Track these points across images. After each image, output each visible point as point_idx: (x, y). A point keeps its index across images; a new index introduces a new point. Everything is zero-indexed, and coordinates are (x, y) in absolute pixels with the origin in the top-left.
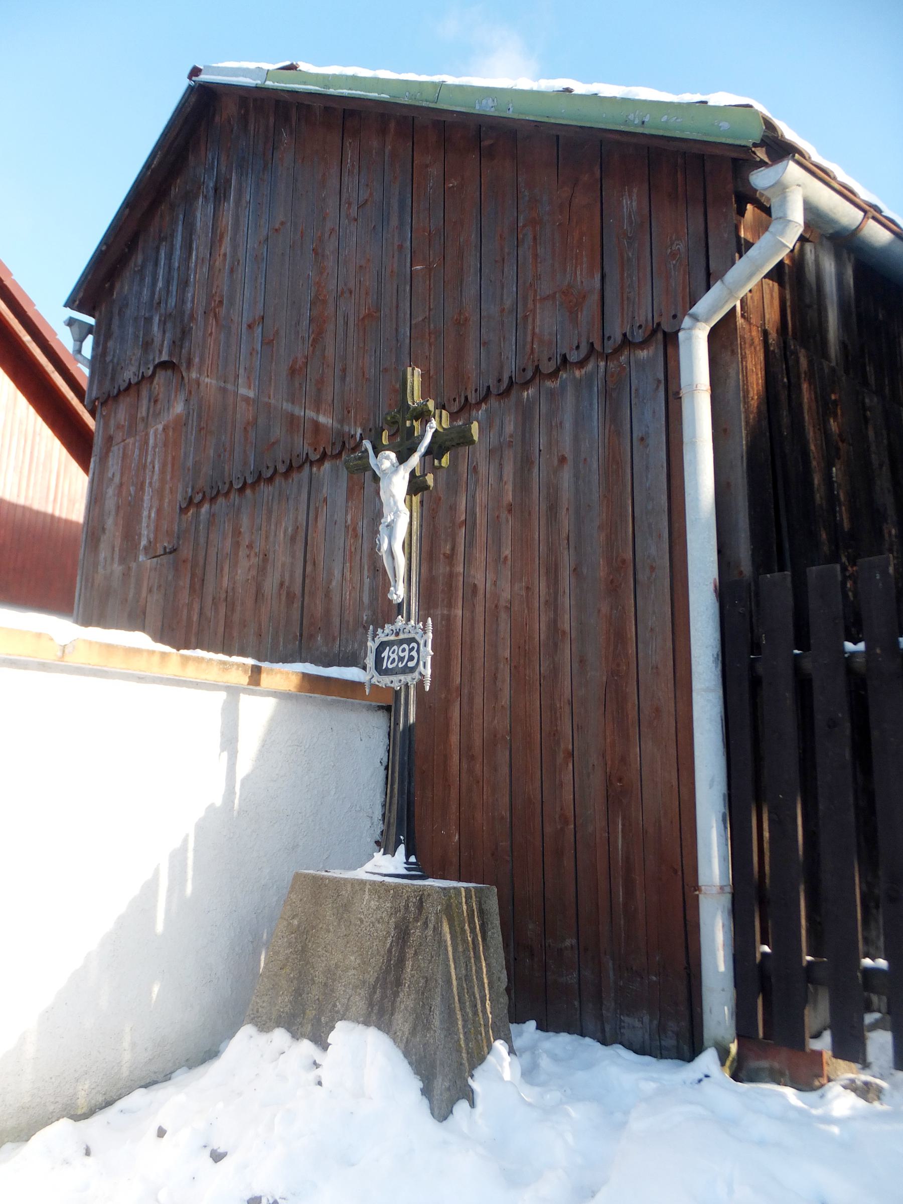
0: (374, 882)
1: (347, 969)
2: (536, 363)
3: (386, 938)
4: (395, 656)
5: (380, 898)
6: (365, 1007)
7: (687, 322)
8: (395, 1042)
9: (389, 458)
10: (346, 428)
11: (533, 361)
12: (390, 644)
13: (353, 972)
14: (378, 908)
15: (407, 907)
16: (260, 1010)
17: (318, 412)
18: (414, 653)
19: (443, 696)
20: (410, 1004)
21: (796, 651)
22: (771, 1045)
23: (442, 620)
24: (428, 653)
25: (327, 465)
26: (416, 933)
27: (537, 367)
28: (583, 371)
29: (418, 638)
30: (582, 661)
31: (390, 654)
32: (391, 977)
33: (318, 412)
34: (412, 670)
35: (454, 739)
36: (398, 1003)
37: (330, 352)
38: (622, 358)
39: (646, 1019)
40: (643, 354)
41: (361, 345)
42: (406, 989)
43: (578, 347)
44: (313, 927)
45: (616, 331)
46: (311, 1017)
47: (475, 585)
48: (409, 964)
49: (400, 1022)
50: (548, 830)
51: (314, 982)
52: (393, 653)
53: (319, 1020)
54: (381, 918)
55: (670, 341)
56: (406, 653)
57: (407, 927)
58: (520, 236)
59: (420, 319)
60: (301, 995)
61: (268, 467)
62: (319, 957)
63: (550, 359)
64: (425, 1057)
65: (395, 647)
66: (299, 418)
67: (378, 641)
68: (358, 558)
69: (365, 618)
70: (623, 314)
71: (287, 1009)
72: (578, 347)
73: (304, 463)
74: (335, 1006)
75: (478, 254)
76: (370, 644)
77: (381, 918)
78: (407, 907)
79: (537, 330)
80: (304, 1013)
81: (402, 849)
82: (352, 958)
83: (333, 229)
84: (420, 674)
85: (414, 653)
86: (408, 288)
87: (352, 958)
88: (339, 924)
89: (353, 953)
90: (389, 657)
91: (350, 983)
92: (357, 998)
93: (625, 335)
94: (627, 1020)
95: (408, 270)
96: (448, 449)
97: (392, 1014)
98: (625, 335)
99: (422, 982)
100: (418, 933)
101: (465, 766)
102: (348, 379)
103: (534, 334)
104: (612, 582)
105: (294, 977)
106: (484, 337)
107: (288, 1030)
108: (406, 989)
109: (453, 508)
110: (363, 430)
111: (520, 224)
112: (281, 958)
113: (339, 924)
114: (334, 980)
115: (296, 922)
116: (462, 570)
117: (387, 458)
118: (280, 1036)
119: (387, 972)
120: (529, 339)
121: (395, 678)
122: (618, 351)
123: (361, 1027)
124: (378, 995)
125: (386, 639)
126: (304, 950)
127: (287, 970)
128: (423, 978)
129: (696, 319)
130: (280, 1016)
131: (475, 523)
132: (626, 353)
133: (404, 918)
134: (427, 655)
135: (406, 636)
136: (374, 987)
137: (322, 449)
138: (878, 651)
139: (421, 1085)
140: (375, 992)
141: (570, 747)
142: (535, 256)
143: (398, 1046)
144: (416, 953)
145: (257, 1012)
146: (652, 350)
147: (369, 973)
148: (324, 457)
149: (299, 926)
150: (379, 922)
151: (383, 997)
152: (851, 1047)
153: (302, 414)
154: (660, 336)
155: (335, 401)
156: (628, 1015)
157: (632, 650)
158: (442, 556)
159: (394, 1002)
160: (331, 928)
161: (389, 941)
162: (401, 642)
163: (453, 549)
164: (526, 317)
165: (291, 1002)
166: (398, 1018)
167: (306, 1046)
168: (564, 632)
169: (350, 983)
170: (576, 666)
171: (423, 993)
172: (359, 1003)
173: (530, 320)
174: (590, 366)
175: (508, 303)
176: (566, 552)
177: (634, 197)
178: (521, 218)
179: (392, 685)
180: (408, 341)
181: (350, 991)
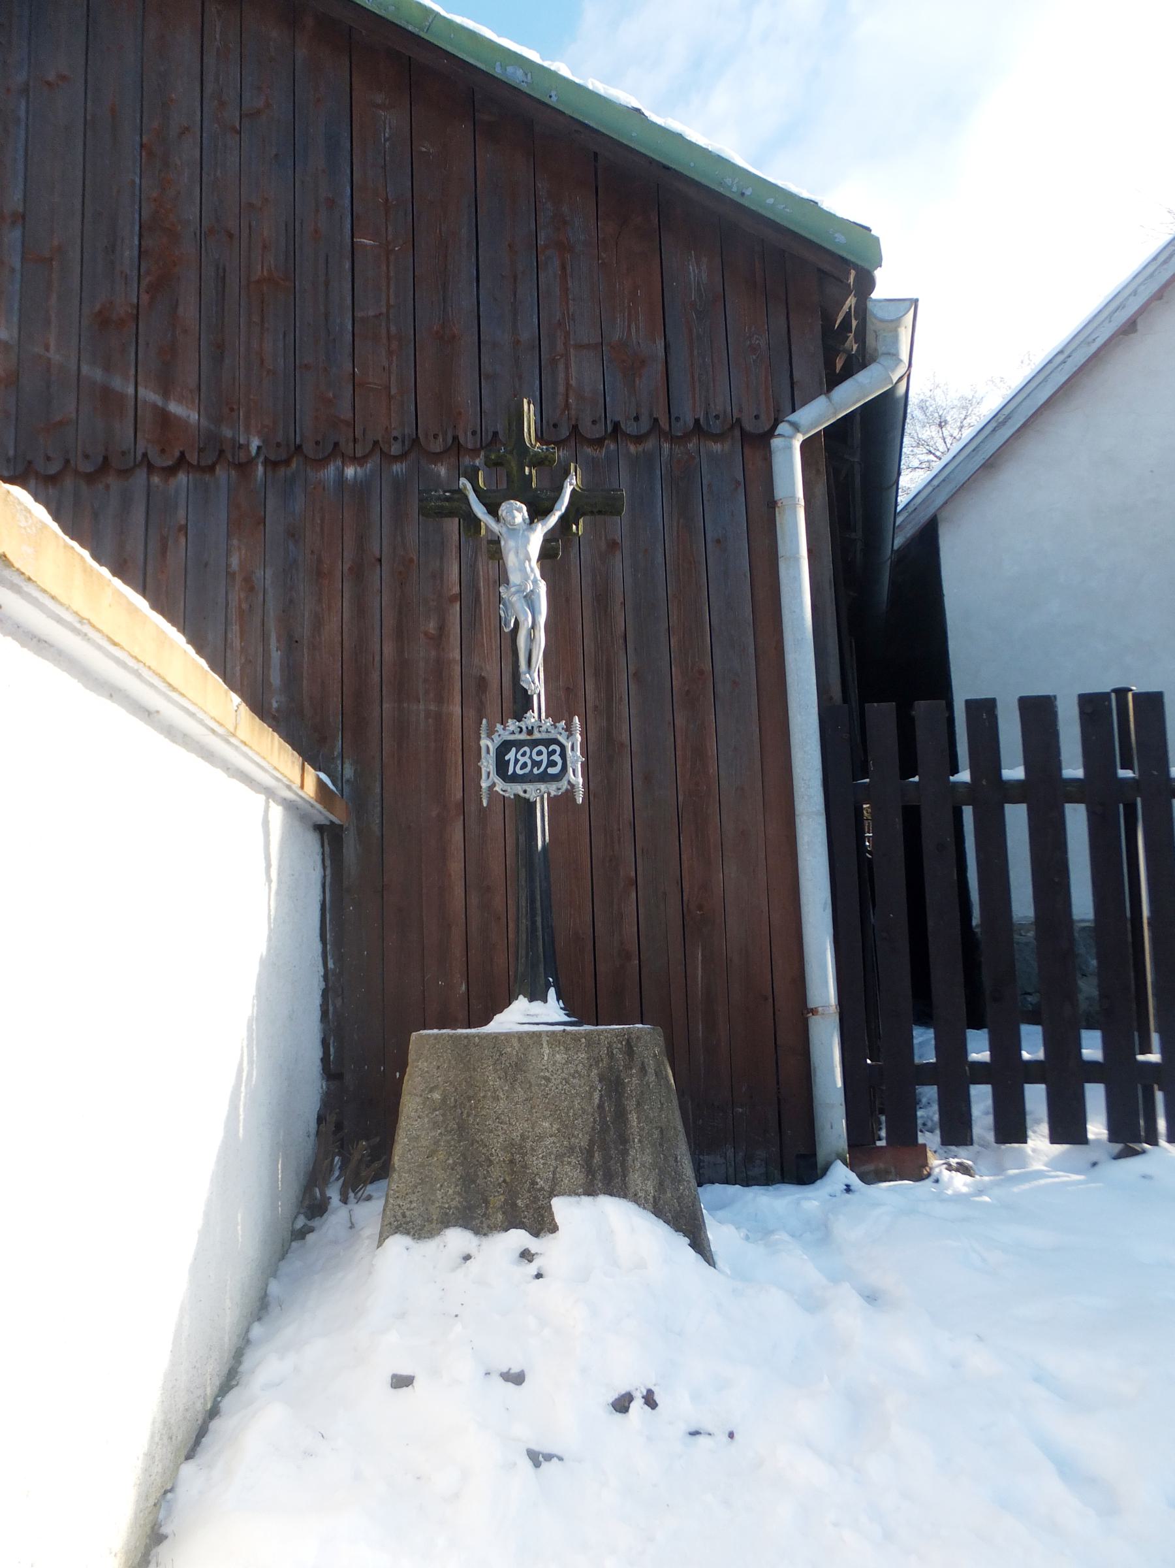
0: (553, 1032)
1: (541, 1138)
2: (573, 423)
3: (591, 1094)
4: (526, 759)
5: (567, 1049)
6: (582, 1176)
7: (783, 428)
8: (639, 1205)
9: (518, 512)
10: (227, 433)
11: (569, 419)
12: (519, 744)
13: (552, 1139)
14: (568, 1062)
15: (611, 1055)
16: (408, 1213)
17: (166, 394)
18: (556, 757)
19: (434, 814)
20: (648, 1159)
21: (916, 779)
22: (886, 1147)
23: (427, 717)
24: (576, 757)
25: (182, 478)
26: (632, 1082)
27: (575, 427)
28: (640, 448)
29: (562, 739)
30: (648, 778)
31: (519, 756)
32: (612, 1135)
33: (166, 394)
34: (556, 778)
35: (456, 866)
36: (630, 1162)
37: (188, 311)
38: (690, 446)
39: (730, 1153)
40: (717, 447)
41: (256, 319)
42: (637, 1145)
43: (637, 419)
44: (469, 1099)
45: (688, 413)
46: (498, 1204)
47: (483, 679)
48: (633, 1118)
49: (639, 1182)
50: (602, 968)
51: (491, 1163)
52: (524, 755)
53: (514, 1205)
54: (576, 1071)
55: (758, 442)
56: (544, 757)
57: (618, 1077)
58: (542, 258)
59: (371, 313)
60: (474, 1182)
61: (48, 459)
62: (491, 1131)
63: (594, 422)
64: (681, 1211)
65: (526, 749)
66: (122, 397)
67: (498, 741)
68: (257, 620)
69: (275, 705)
70: (694, 397)
71: (454, 1204)
72: (637, 419)
73: (135, 466)
74: (534, 1183)
75: (474, 259)
76: (484, 742)
77: (576, 1071)
78: (611, 1055)
79: (573, 382)
80: (486, 1202)
81: (552, 992)
82: (547, 1125)
83: (187, 129)
84: (569, 782)
85: (556, 757)
86: (347, 265)
87: (547, 1125)
88: (513, 1088)
89: (545, 1118)
90: (517, 761)
91: (551, 1153)
92: (567, 1168)
93: (697, 421)
94: (706, 1158)
95: (349, 241)
96: (583, 514)
97: (625, 1176)
98: (697, 421)
99: (656, 1134)
100: (635, 1081)
101: (474, 900)
102: (227, 361)
103: (568, 386)
104: (688, 692)
105: (455, 1163)
106: (487, 368)
107: (466, 1226)
108: (637, 1145)
109: (439, 576)
110: (265, 441)
111: (541, 242)
112: (425, 1143)
113: (513, 1088)
114: (524, 1155)
115: (437, 1096)
116: (458, 658)
117: (519, 510)
118: (457, 1239)
119: (604, 1130)
120: (561, 389)
121: (529, 787)
122: (686, 437)
123: (586, 1200)
124: (597, 1158)
125: (512, 737)
126: (462, 1127)
127: (441, 1155)
128: (656, 1128)
129: (796, 427)
130: (447, 1214)
131: (477, 600)
132: (695, 440)
133: (611, 1068)
134: (577, 761)
135: (545, 736)
136: (590, 1153)
137: (177, 454)
138: (984, 783)
139: (687, 1241)
140: (592, 1157)
141: (633, 874)
142: (565, 290)
143: (645, 1208)
144: (638, 1104)
145: (404, 1216)
146: (727, 446)
147: (577, 1137)
148: (182, 462)
149: (444, 1100)
150: (574, 1077)
151: (607, 1158)
152: (957, 1132)
153: (131, 390)
154: (737, 433)
155: (203, 387)
156: (708, 1154)
157: (712, 770)
158: (422, 636)
159: (623, 1164)
160: (501, 1095)
161: (596, 1095)
162: (534, 743)
163: (442, 628)
164: (554, 362)
165: (459, 1194)
166: (635, 1179)
167: (518, 1238)
168: (622, 745)
169: (551, 1153)
170: (638, 784)
171: (661, 1145)
172: (573, 1173)
173: (561, 366)
174: (650, 444)
175: (525, 336)
176: (622, 653)
177: (704, 267)
178: (542, 236)
179: (527, 796)
180: (349, 337)
181: (554, 1163)
